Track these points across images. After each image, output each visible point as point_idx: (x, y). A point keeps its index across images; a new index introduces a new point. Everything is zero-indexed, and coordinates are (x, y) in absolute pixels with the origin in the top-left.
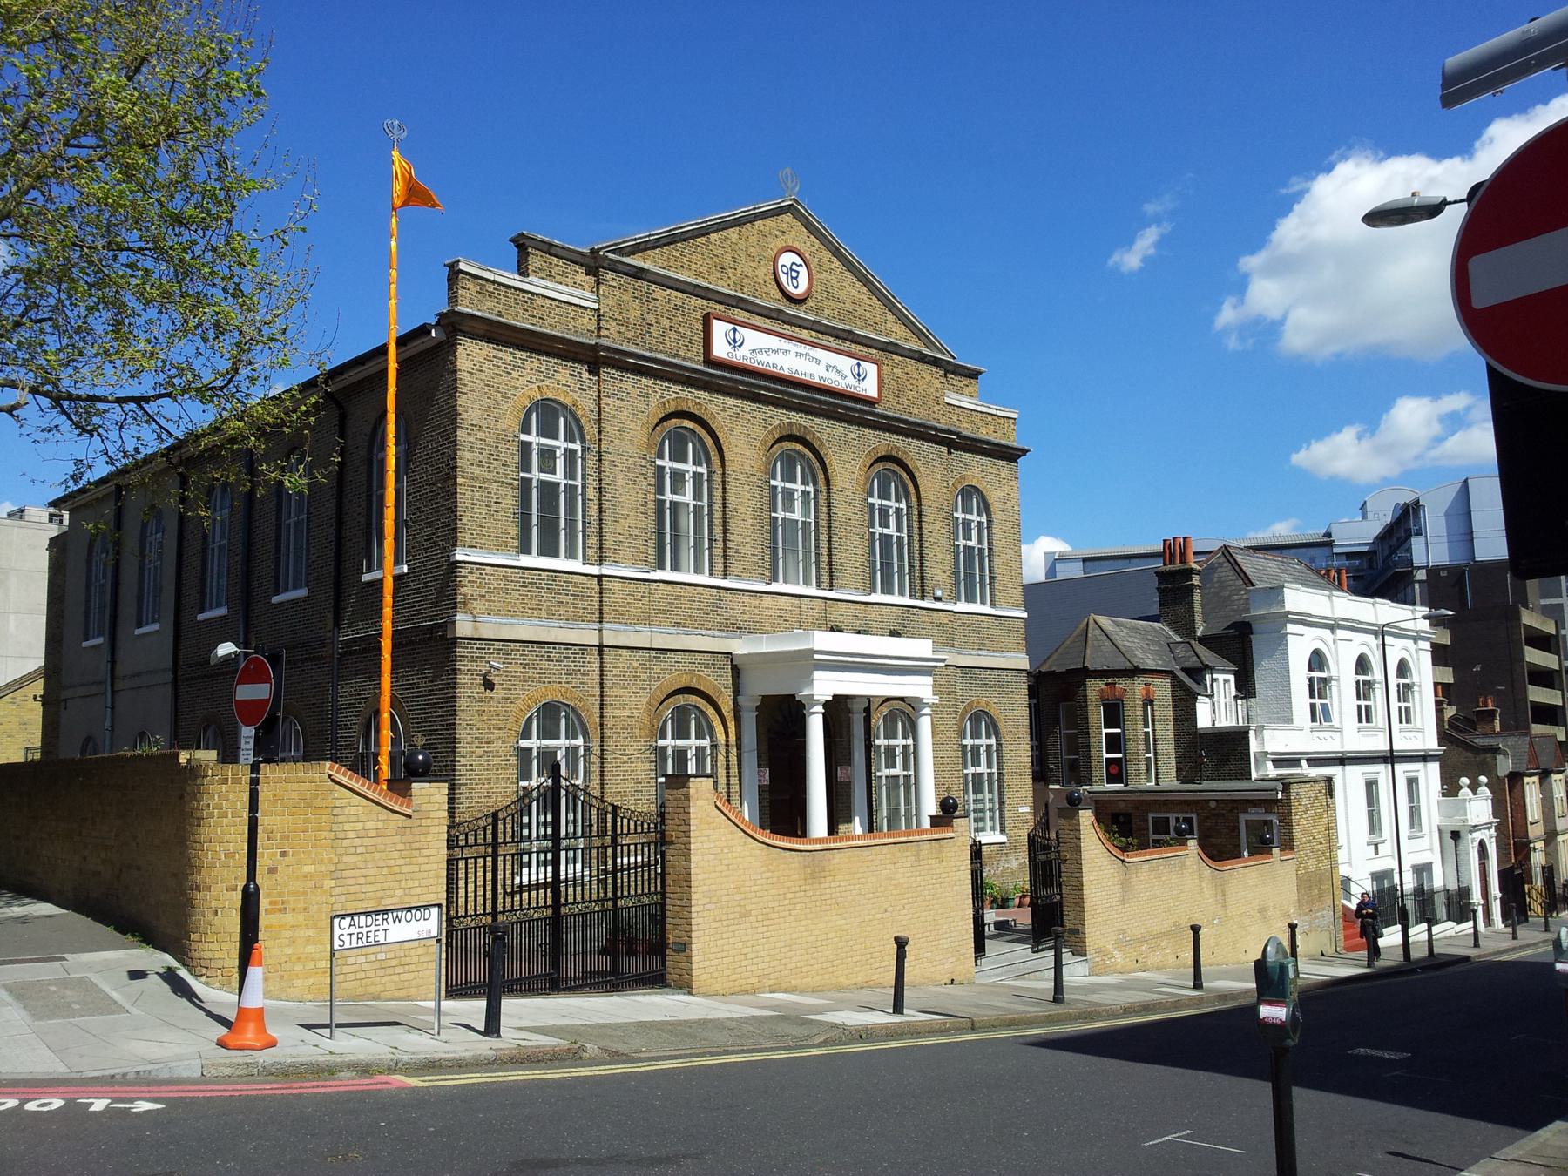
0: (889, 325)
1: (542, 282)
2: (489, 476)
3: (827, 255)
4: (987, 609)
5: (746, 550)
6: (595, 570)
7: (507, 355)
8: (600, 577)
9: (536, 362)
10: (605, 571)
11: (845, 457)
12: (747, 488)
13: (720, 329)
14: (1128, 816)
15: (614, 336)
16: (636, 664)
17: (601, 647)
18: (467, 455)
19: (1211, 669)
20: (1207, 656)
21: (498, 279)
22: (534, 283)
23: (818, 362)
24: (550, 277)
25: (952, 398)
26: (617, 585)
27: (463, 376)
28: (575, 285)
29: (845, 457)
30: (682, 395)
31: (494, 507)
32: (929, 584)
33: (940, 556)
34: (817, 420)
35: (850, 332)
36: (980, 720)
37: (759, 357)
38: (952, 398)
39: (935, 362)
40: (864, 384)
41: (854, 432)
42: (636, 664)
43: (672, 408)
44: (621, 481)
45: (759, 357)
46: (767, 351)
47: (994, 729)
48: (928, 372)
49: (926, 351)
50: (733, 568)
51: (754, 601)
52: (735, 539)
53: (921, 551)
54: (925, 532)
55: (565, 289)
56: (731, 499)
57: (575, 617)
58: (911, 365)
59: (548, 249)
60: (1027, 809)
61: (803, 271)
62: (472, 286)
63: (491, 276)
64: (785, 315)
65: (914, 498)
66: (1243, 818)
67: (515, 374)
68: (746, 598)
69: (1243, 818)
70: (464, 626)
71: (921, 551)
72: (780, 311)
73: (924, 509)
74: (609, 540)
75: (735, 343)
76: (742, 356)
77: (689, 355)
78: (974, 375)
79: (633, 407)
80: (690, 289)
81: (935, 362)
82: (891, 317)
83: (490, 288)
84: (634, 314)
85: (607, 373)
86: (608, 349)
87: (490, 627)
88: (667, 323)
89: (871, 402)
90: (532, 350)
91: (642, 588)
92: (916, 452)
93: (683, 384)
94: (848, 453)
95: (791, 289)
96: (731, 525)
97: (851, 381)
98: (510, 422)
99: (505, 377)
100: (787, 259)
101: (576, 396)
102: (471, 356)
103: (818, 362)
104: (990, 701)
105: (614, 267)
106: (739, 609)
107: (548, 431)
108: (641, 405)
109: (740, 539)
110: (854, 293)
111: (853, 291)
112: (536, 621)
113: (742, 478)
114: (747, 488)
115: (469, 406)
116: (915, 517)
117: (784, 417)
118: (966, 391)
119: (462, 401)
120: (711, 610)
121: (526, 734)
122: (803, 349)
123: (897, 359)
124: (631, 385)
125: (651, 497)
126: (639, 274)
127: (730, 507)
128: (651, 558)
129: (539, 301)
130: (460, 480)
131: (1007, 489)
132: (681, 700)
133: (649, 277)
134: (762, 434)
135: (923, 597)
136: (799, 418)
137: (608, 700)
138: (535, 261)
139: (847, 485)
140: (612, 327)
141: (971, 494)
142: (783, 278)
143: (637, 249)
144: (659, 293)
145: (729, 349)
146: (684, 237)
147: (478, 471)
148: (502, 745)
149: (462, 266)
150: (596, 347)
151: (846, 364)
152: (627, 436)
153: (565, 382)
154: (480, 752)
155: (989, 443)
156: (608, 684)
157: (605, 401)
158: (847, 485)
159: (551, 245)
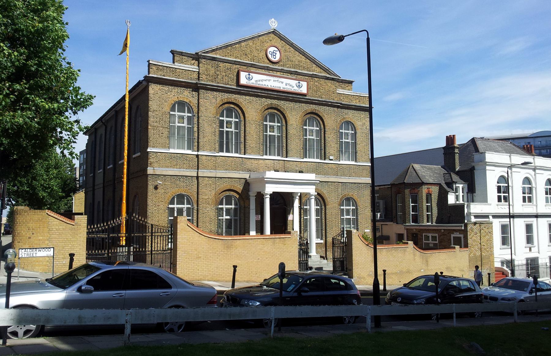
0: (313, 68)
1: (179, 65)
3: (288, 47)
4: (353, 163)
5: (254, 145)
6: (196, 153)
7: (166, 88)
8: (197, 156)
9: (176, 90)
10: (199, 153)
11: (293, 114)
12: (254, 125)
13: (243, 75)
14: (416, 234)
15: (204, 81)
16: (210, 182)
17: (197, 177)
18: (152, 119)
19: (456, 183)
20: (455, 178)
21: (163, 65)
22: (177, 65)
23: (282, 83)
24: (182, 62)
25: (340, 91)
26: (204, 157)
27: (151, 95)
28: (191, 64)
29: (293, 114)
30: (229, 97)
31: (161, 135)
32: (327, 155)
33: (333, 145)
34: (282, 102)
35: (296, 72)
36: (349, 200)
37: (259, 83)
38: (340, 91)
39: (333, 79)
40: (301, 89)
41: (297, 105)
42: (210, 182)
44: (206, 125)
46: (262, 81)
47: (355, 204)
48: (329, 83)
49: (328, 76)
50: (248, 151)
51: (256, 162)
52: (249, 142)
53: (325, 144)
54: (327, 138)
55: (188, 66)
56: (247, 129)
57: (189, 167)
58: (322, 81)
59: (181, 54)
60: (369, 231)
61: (278, 53)
62: (154, 68)
63: (161, 64)
64: (271, 68)
65: (322, 126)
66: (452, 236)
67: (169, 94)
68: (253, 161)
69: (452, 236)
70: (150, 171)
71: (325, 144)
72: (268, 67)
73: (326, 130)
74: (201, 144)
75: (249, 79)
76: (252, 83)
77: (232, 84)
78: (351, 82)
79: (210, 103)
81: (333, 79)
82: (314, 65)
83: (161, 68)
84: (212, 71)
85: (202, 92)
86: (201, 84)
87: (159, 171)
88: (224, 74)
89: (305, 95)
90: (175, 86)
91: (213, 158)
92: (321, 110)
93: (230, 93)
94: (295, 114)
95: (273, 59)
96: (247, 138)
97: (296, 88)
98: (167, 108)
99: (166, 95)
100: (271, 49)
102: (153, 89)
103: (282, 83)
104: (354, 194)
106: (249, 164)
107: (181, 110)
108: (214, 101)
109: (251, 142)
110: (299, 58)
112: (176, 169)
113: (252, 122)
114: (254, 125)
115: (153, 104)
116: (323, 133)
117: (269, 101)
118: (347, 88)
119: (150, 103)
120: (240, 165)
121: (172, 202)
122: (276, 79)
123: (316, 79)
124: (210, 95)
125: (217, 130)
126: (214, 59)
127: (247, 132)
128: (217, 149)
129: (178, 70)
130: (149, 127)
131: (364, 121)
132: (228, 193)
134: (260, 108)
135: (325, 160)
136: (275, 102)
137: (200, 193)
138: (177, 58)
139: (294, 123)
140: (204, 77)
141: (349, 124)
142: (270, 56)
144: (221, 64)
145: (247, 81)
147: (155, 124)
148: (163, 206)
149: (151, 62)
150: (197, 84)
151: (294, 83)
152: (208, 111)
153: (187, 95)
155: (355, 106)
156: (200, 188)
157: (200, 100)
158: (294, 123)
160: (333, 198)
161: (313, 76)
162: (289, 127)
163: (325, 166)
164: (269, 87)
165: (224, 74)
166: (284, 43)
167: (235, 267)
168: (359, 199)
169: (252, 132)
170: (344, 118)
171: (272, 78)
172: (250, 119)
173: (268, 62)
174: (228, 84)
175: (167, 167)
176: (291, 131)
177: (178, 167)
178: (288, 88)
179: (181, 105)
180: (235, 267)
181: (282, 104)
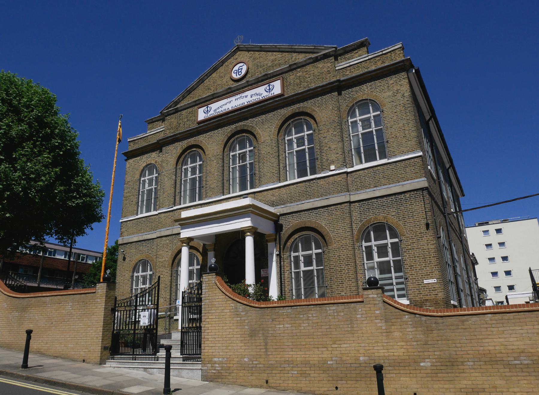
2: (130, 195)
11: (267, 127)
16: (168, 241)
22: (149, 133)
24: (153, 128)
29: (267, 127)
33: (333, 147)
37: (218, 111)
39: (326, 56)
41: (270, 115)
43: (186, 146)
44: (166, 179)
45: (218, 111)
48: (320, 65)
49: (314, 56)
63: (136, 138)
76: (212, 113)
80: (194, 104)
83: (136, 141)
91: (171, 213)
103: (246, 96)
104: (389, 215)
105: (169, 114)
113: (213, 159)
114: (215, 161)
123: (299, 70)
129: (149, 137)
133: (180, 109)
143: (177, 103)
146: (193, 89)
148: (128, 275)
154: (122, 278)
159: (152, 119)
160: (340, 231)
161: (293, 68)
163: (322, 182)
165: (186, 120)
166: (252, 53)
167: (29, 333)
168: (401, 223)
169: (213, 170)
171: (233, 98)
172: (210, 156)
175: (133, 234)
177: (142, 231)
179: (150, 167)
180: (29, 333)
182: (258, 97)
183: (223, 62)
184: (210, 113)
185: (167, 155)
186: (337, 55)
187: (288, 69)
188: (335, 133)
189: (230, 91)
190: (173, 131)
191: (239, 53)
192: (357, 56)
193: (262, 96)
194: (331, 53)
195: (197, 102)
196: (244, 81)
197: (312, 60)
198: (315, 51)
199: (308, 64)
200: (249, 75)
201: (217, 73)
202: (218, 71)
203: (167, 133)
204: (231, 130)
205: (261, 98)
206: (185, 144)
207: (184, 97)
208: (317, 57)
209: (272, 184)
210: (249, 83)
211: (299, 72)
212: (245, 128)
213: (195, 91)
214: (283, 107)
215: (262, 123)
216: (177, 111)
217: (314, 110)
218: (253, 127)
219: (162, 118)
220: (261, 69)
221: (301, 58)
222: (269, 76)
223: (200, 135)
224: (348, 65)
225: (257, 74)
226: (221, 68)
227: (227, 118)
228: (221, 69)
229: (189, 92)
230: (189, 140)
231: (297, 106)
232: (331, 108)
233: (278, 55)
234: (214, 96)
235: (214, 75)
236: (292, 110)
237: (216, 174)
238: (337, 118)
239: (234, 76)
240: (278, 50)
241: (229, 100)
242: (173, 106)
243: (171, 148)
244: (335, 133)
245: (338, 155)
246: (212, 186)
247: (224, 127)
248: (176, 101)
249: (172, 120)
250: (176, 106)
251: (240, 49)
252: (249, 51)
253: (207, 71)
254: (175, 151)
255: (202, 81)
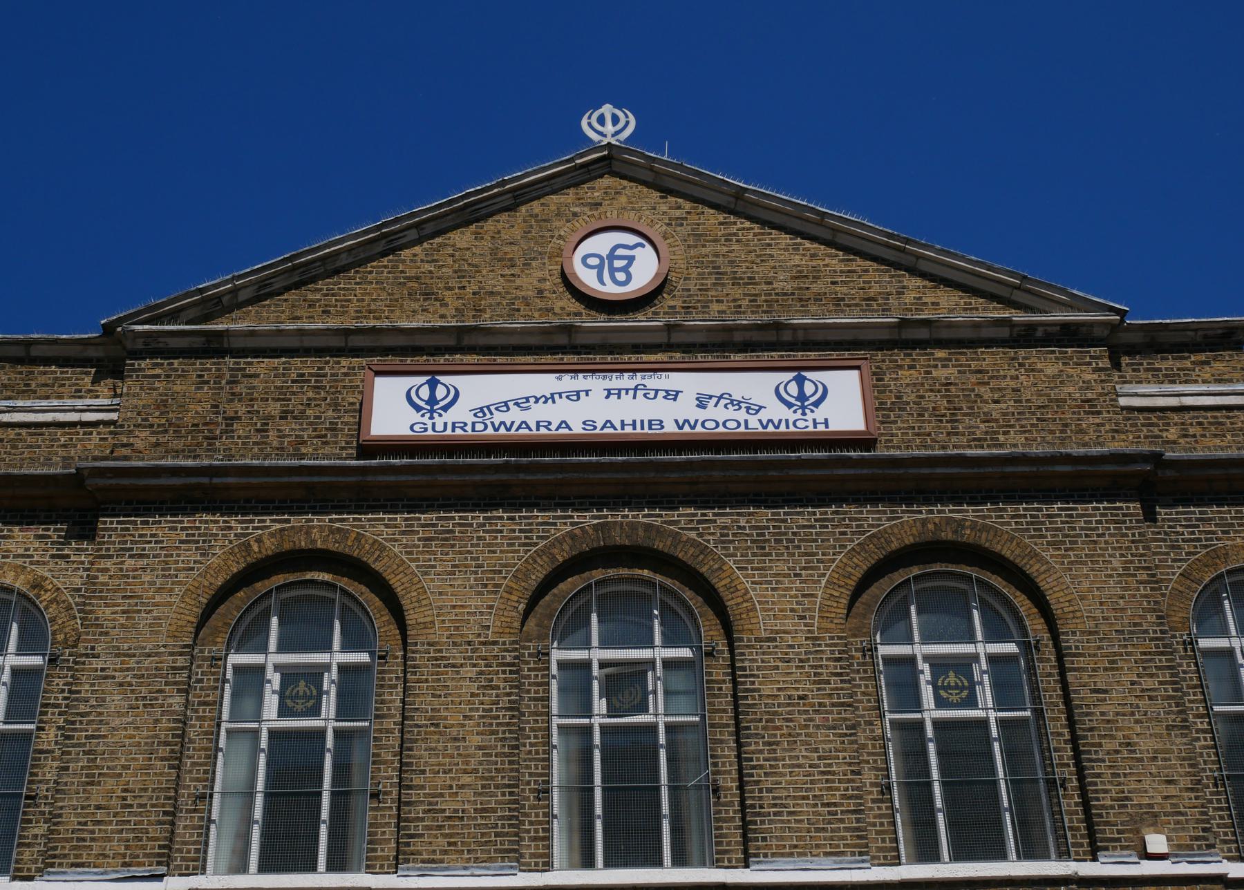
3: (712, 217)
11: (782, 567)
23: (673, 395)
24: (26, 393)
29: (782, 567)
32: (1112, 817)
33: (1146, 745)
35: (778, 326)
37: (498, 417)
39: (1069, 336)
41: (801, 518)
43: (270, 546)
44: (115, 701)
48: (1048, 363)
54: (1082, 696)
58: (988, 358)
72: (568, 329)
73: (1071, 641)
79: (163, 568)
88: (275, 409)
101: (42, 571)
103: (673, 395)
105: (155, 348)
111: (786, 257)
113: (455, 655)
118: (1206, 372)
123: (941, 354)
133: (238, 343)
134: (517, 559)
143: (215, 306)
144: (261, 367)
145: (415, 417)
146: (332, 267)
152: (143, 620)
159: (29, 344)
161: (909, 338)
162: (751, 659)
164: (578, 429)
165: (275, 409)
166: (688, 205)
169: (453, 718)
170: (1217, 555)
171: (596, 384)
172: (438, 634)
173: (575, 306)
174: (302, 456)
176: (771, 679)
178: (721, 420)
181: (681, 526)
182: (741, 415)
183: (519, 197)
184: (451, 416)
185: (130, 563)
186: (1126, 346)
187: (885, 335)
188: (1148, 683)
189: (562, 340)
190: (179, 444)
191: (607, 181)
192: (1207, 376)
193: (764, 416)
194: (1098, 332)
195: (357, 341)
196: (640, 320)
197: (1004, 333)
198: (1019, 297)
199: (989, 343)
200: (668, 301)
201: (478, 236)
202: (489, 226)
203: (139, 444)
204: (571, 535)
205: (754, 423)
206: (267, 531)
207: (264, 292)
208: (1031, 327)
209: (828, 862)
210: (677, 338)
211: (945, 363)
212: (659, 545)
213: (341, 282)
214: (874, 501)
215: (760, 543)
216: (215, 347)
217: (1041, 560)
218: (704, 550)
219: (109, 359)
220: (738, 292)
221: (947, 306)
222: (787, 336)
223: (374, 509)
224: (1173, 402)
225: (715, 307)
226: (504, 216)
227: (561, 467)
228: (507, 228)
229: (303, 276)
230: (297, 521)
231: (969, 512)
232: (1116, 563)
233: (833, 261)
234: (467, 341)
235: (461, 238)
236: (928, 522)
237: (476, 740)
238: (1151, 618)
239: (587, 278)
240: (827, 235)
241: (568, 383)
242: (192, 313)
243: (164, 530)
244: (1148, 683)
245: (1172, 790)
246: (447, 804)
247: (530, 506)
248: (219, 297)
249: (190, 389)
250: (206, 319)
251: (616, 166)
252: (666, 191)
253: (426, 207)
254: (188, 556)
255: (388, 244)
